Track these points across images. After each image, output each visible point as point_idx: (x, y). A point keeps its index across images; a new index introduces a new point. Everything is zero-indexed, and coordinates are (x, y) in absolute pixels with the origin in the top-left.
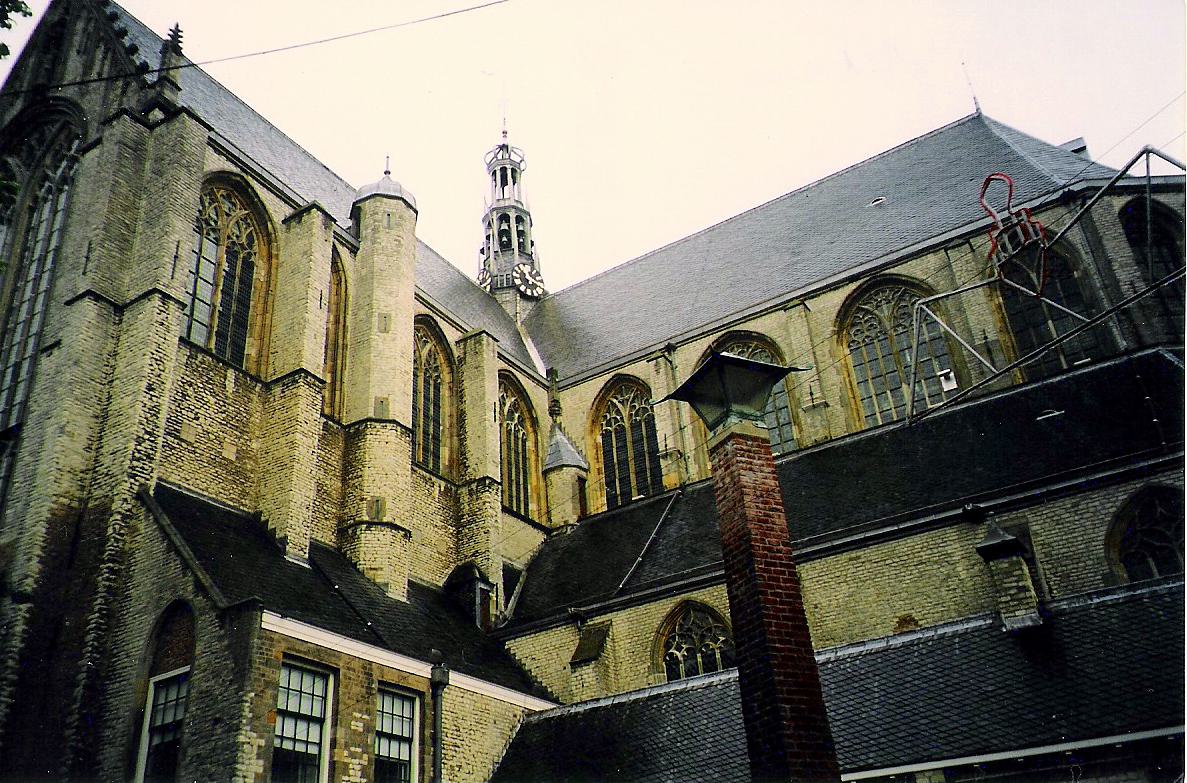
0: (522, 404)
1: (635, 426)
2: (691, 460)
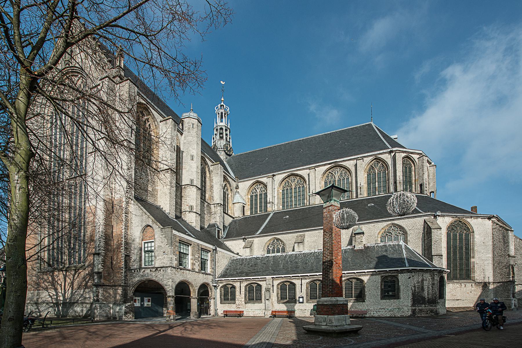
0: (228, 185)
1: (261, 195)
2: (276, 205)
